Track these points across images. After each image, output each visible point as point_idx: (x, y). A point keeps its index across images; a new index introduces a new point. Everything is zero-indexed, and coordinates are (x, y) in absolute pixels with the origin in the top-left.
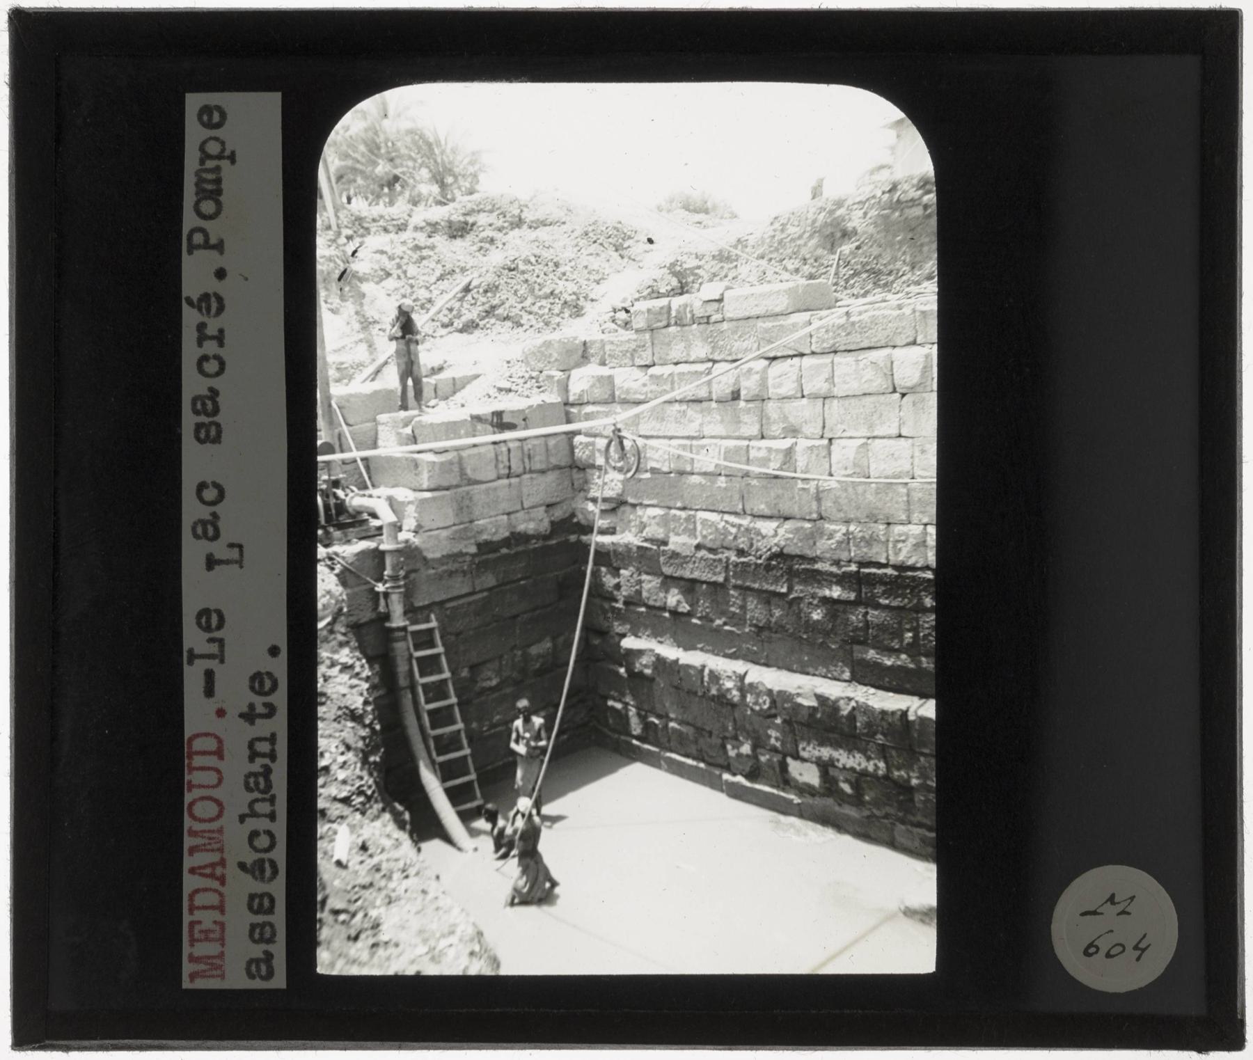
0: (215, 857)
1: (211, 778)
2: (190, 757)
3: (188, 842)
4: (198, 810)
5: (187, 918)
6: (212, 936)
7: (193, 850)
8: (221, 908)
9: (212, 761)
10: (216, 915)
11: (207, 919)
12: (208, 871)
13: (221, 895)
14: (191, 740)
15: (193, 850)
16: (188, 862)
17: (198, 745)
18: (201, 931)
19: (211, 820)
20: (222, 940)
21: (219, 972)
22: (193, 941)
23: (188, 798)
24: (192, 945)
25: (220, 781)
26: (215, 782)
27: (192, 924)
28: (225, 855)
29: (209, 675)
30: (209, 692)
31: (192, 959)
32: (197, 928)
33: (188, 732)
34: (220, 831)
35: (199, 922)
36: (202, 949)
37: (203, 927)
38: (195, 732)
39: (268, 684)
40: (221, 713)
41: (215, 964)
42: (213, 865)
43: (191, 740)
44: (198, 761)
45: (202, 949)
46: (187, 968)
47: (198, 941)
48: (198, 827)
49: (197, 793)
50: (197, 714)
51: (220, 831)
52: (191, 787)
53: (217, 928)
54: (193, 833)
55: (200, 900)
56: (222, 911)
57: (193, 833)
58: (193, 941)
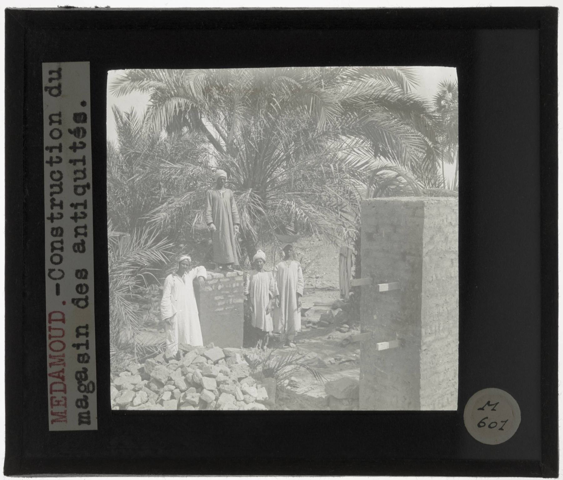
0: (60, 368)
1: (60, 333)
2: (50, 322)
3: (49, 361)
4: (54, 346)
5: (49, 396)
6: (61, 403)
7: (51, 365)
8: (64, 391)
9: (59, 325)
10: (62, 394)
11: (59, 396)
12: (57, 375)
13: (65, 385)
14: (50, 315)
15: (51, 365)
16: (50, 370)
17: (54, 317)
18: (56, 401)
19: (61, 350)
20: (65, 405)
21: (64, 419)
22: (52, 405)
23: (48, 341)
24: (52, 408)
25: (64, 332)
26: (61, 335)
27: (52, 398)
28: (66, 368)
29: (58, 286)
30: (58, 293)
31: (53, 414)
32: (54, 400)
33: (48, 310)
34: (64, 356)
35: (55, 397)
36: (56, 409)
37: (57, 399)
38: (52, 311)
39: (84, 289)
40: (64, 303)
41: (63, 416)
42: (61, 371)
43: (50, 315)
44: (54, 325)
45: (56, 409)
46: (51, 418)
47: (55, 405)
48: (54, 354)
49: (53, 339)
50: (52, 303)
51: (64, 356)
52: (50, 337)
53: (63, 399)
54: (50, 357)
55: (55, 387)
56: (65, 393)
57: (50, 357)
58: (52, 405)
